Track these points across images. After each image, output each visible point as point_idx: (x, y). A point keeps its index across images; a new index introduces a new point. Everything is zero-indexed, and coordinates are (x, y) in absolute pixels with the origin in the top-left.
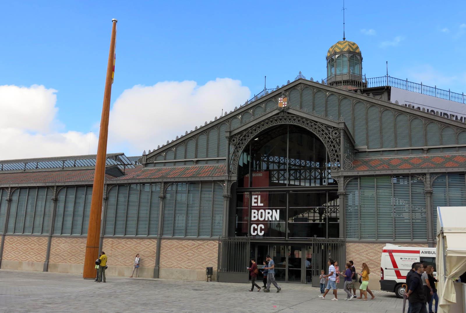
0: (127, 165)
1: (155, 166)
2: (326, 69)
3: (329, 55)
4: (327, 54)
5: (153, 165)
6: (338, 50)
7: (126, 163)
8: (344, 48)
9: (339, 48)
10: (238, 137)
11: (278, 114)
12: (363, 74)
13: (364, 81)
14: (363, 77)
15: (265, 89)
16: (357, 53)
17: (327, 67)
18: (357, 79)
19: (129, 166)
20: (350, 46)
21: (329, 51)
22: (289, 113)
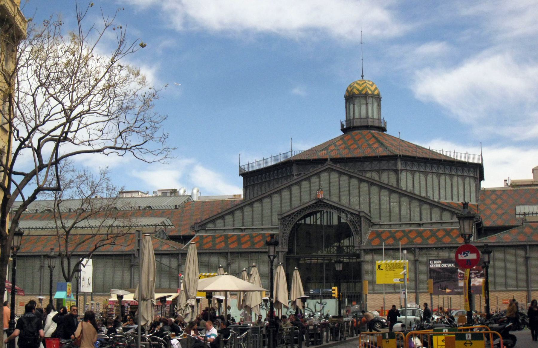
0: (168, 226)
1: (206, 232)
2: (345, 109)
3: (347, 95)
4: (343, 93)
5: (204, 231)
6: (357, 92)
7: (167, 224)
8: (363, 90)
9: (358, 90)
10: (286, 218)
11: (316, 203)
12: (382, 118)
13: (383, 126)
14: (382, 121)
15: (291, 151)
16: (375, 95)
17: (346, 107)
18: (376, 124)
19: (169, 227)
20: (369, 88)
21: (347, 91)
22: (324, 203)
